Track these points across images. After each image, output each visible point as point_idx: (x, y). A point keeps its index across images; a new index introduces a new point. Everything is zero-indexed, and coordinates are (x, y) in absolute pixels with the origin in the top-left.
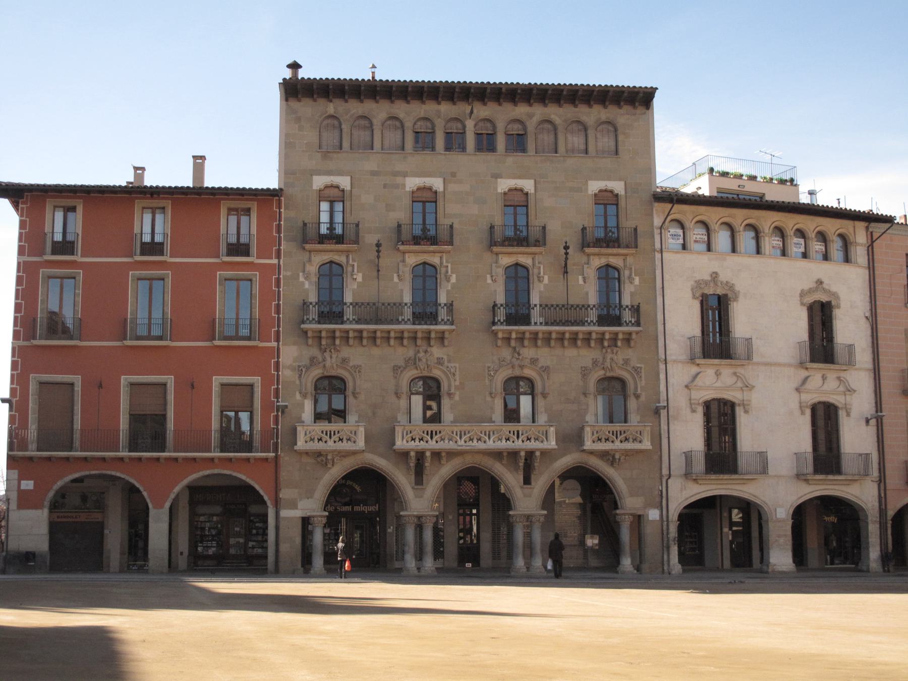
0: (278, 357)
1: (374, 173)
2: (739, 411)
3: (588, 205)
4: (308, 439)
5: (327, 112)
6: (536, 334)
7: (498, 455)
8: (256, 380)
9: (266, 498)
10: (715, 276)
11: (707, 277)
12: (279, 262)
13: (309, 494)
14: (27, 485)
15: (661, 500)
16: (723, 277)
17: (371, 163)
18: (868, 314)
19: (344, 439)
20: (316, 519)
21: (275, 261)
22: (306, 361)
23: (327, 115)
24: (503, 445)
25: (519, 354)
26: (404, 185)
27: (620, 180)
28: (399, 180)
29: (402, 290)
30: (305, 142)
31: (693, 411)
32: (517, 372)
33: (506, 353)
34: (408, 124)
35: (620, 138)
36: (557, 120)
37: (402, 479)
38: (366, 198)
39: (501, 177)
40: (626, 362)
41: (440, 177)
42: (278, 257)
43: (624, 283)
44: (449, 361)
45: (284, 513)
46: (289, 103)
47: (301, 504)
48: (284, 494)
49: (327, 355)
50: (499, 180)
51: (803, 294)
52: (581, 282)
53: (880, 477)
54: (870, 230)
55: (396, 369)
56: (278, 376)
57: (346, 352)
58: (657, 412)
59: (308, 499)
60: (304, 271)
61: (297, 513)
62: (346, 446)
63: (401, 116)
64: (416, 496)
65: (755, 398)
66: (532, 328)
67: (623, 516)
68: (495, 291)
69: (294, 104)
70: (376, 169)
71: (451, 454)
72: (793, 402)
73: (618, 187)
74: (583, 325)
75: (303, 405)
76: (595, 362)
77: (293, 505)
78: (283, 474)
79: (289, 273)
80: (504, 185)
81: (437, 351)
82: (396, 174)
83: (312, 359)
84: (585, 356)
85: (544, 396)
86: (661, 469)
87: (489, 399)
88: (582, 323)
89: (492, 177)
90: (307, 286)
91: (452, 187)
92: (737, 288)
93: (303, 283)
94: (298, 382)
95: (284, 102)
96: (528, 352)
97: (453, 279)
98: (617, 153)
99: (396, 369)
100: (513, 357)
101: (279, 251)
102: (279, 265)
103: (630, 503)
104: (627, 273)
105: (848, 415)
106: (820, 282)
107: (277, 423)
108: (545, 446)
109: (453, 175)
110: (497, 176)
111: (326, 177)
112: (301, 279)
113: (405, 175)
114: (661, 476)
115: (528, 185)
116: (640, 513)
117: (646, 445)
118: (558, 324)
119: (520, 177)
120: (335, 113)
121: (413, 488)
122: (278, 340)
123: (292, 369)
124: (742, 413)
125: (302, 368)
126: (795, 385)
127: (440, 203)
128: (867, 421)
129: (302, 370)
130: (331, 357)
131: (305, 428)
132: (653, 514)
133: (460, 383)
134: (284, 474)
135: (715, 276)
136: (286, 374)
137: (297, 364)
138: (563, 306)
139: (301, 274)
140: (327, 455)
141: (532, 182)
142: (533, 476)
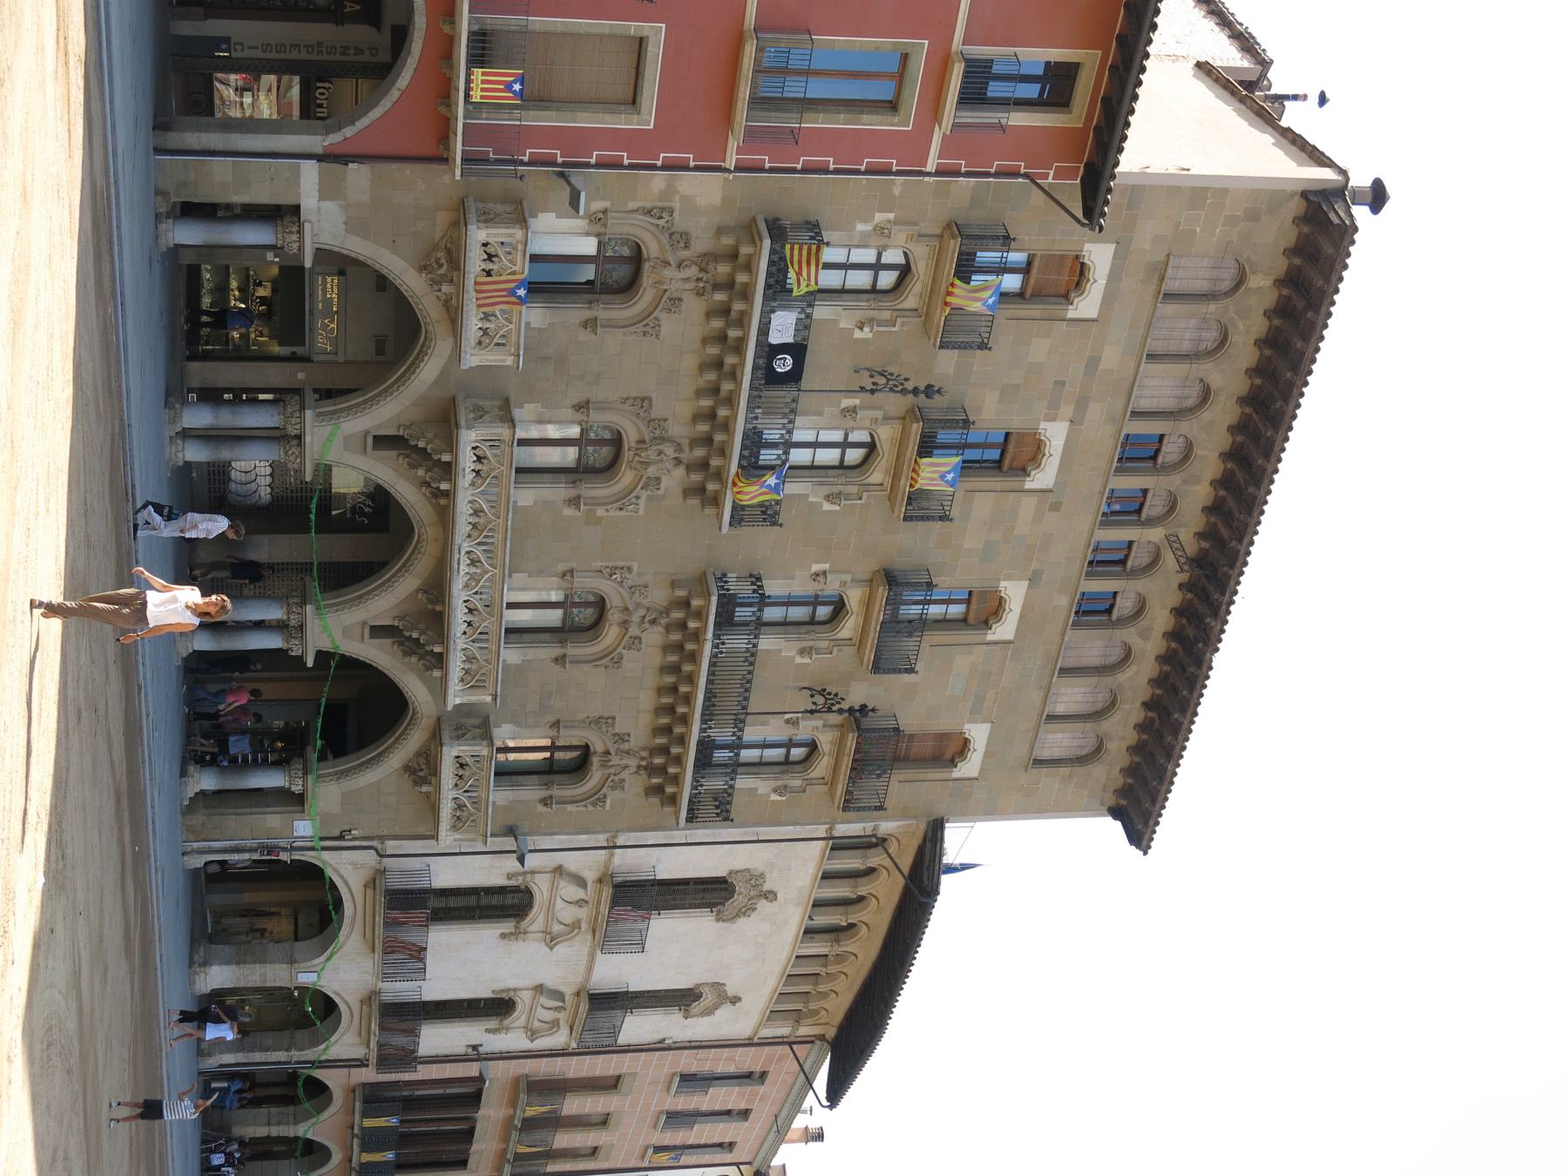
0: (698, 168)
1: (1093, 364)
2: (507, 926)
3: (943, 724)
4: (491, 250)
5: (1254, 273)
7: (437, 588)
8: (647, 119)
9: (349, 132)
12: (929, 174)
13: (355, 225)
15: (338, 839)
17: (1113, 357)
19: (487, 325)
20: (295, 237)
21: (931, 166)
22: (680, 221)
23: (1248, 271)
24: (458, 595)
25: (653, 622)
26: (1053, 418)
27: (982, 771)
28: (1068, 409)
29: (820, 414)
30: (1198, 230)
33: (659, 596)
34: (1184, 426)
35: (1064, 771)
36: (1123, 677)
37: (385, 413)
38: (1039, 350)
39: (1030, 587)
40: (620, 785)
41: (1056, 483)
43: (775, 779)
44: (649, 499)
45: (310, 170)
46: (1297, 198)
47: (330, 206)
48: (358, 176)
49: (693, 271)
50: (1025, 583)
54: (818, 1042)
55: (644, 401)
56: (653, 167)
57: (694, 307)
58: (511, 831)
59: (345, 223)
60: (895, 223)
62: (473, 325)
63: (1207, 415)
64: (347, 439)
67: (300, 783)
68: (793, 578)
69: (1296, 207)
70: (1100, 368)
71: (445, 516)
74: (704, 721)
76: (622, 738)
77: (327, 191)
79: (897, 191)
80: (1015, 593)
81: (674, 479)
82: (1082, 404)
83: (685, 239)
84: (637, 721)
85: (560, 660)
86: (395, 837)
87: (562, 567)
88: (707, 716)
89: (1035, 572)
90: (860, 227)
91: (1028, 505)
93: (865, 220)
94: (632, 205)
95: (1301, 188)
96: (654, 637)
98: (1039, 762)
99: (644, 401)
100: (648, 609)
101: (956, 173)
102: (921, 173)
104: (797, 783)
108: (454, 685)
109: (1055, 507)
110: (1034, 580)
111: (1107, 271)
112: (879, 217)
114: (382, 838)
118: (706, 699)
119: (1022, 616)
120: (1250, 289)
121: (367, 433)
122: (739, 168)
123: (669, 191)
124: (500, 931)
125: (667, 218)
127: (998, 482)
129: (661, 218)
130: (687, 280)
131: (520, 247)
132: (304, 828)
133: (602, 518)
134: (408, 172)
136: (659, 180)
137: (677, 206)
138: (744, 708)
139: (891, 216)
140: (452, 281)
141: (1010, 636)
142: (390, 641)
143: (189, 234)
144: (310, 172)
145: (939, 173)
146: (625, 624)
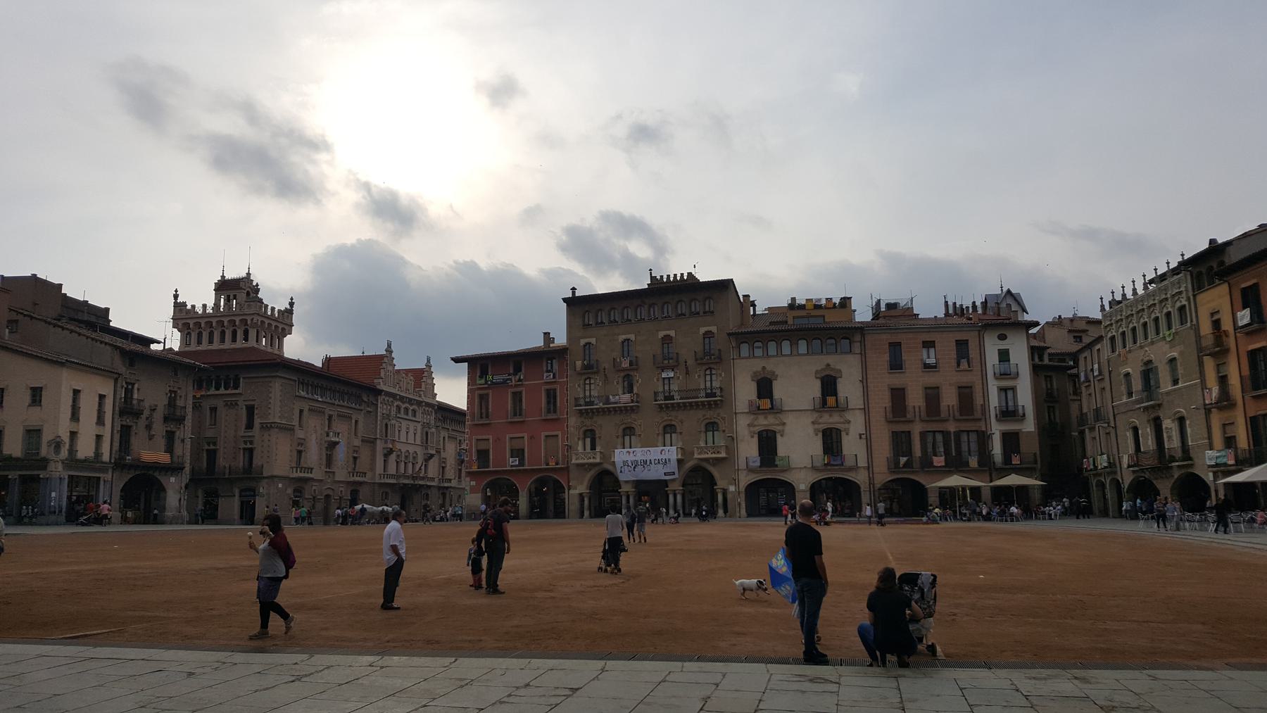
6: (678, 404)
8: (559, 433)
9: (564, 485)
10: (764, 368)
11: (760, 369)
14: (473, 483)
15: (735, 482)
16: (768, 368)
18: (860, 379)
26: (618, 340)
31: (752, 437)
32: (668, 423)
42: (567, 378)
51: (817, 372)
52: (696, 377)
53: (869, 467)
61: (577, 492)
65: (787, 429)
66: (675, 401)
72: (810, 430)
73: (714, 329)
75: (578, 444)
78: (571, 476)
80: (661, 334)
81: (633, 416)
92: (776, 373)
97: (640, 382)
103: (721, 484)
105: (847, 434)
106: (828, 365)
107: (568, 452)
110: (657, 331)
113: (619, 334)
115: (672, 333)
116: (726, 488)
117: (723, 455)
122: (567, 415)
126: (813, 420)
128: (860, 435)
132: (732, 488)
135: (764, 368)
143: (586, 513)
144: (571, 492)
145: (567, 378)
146: (671, 420)
